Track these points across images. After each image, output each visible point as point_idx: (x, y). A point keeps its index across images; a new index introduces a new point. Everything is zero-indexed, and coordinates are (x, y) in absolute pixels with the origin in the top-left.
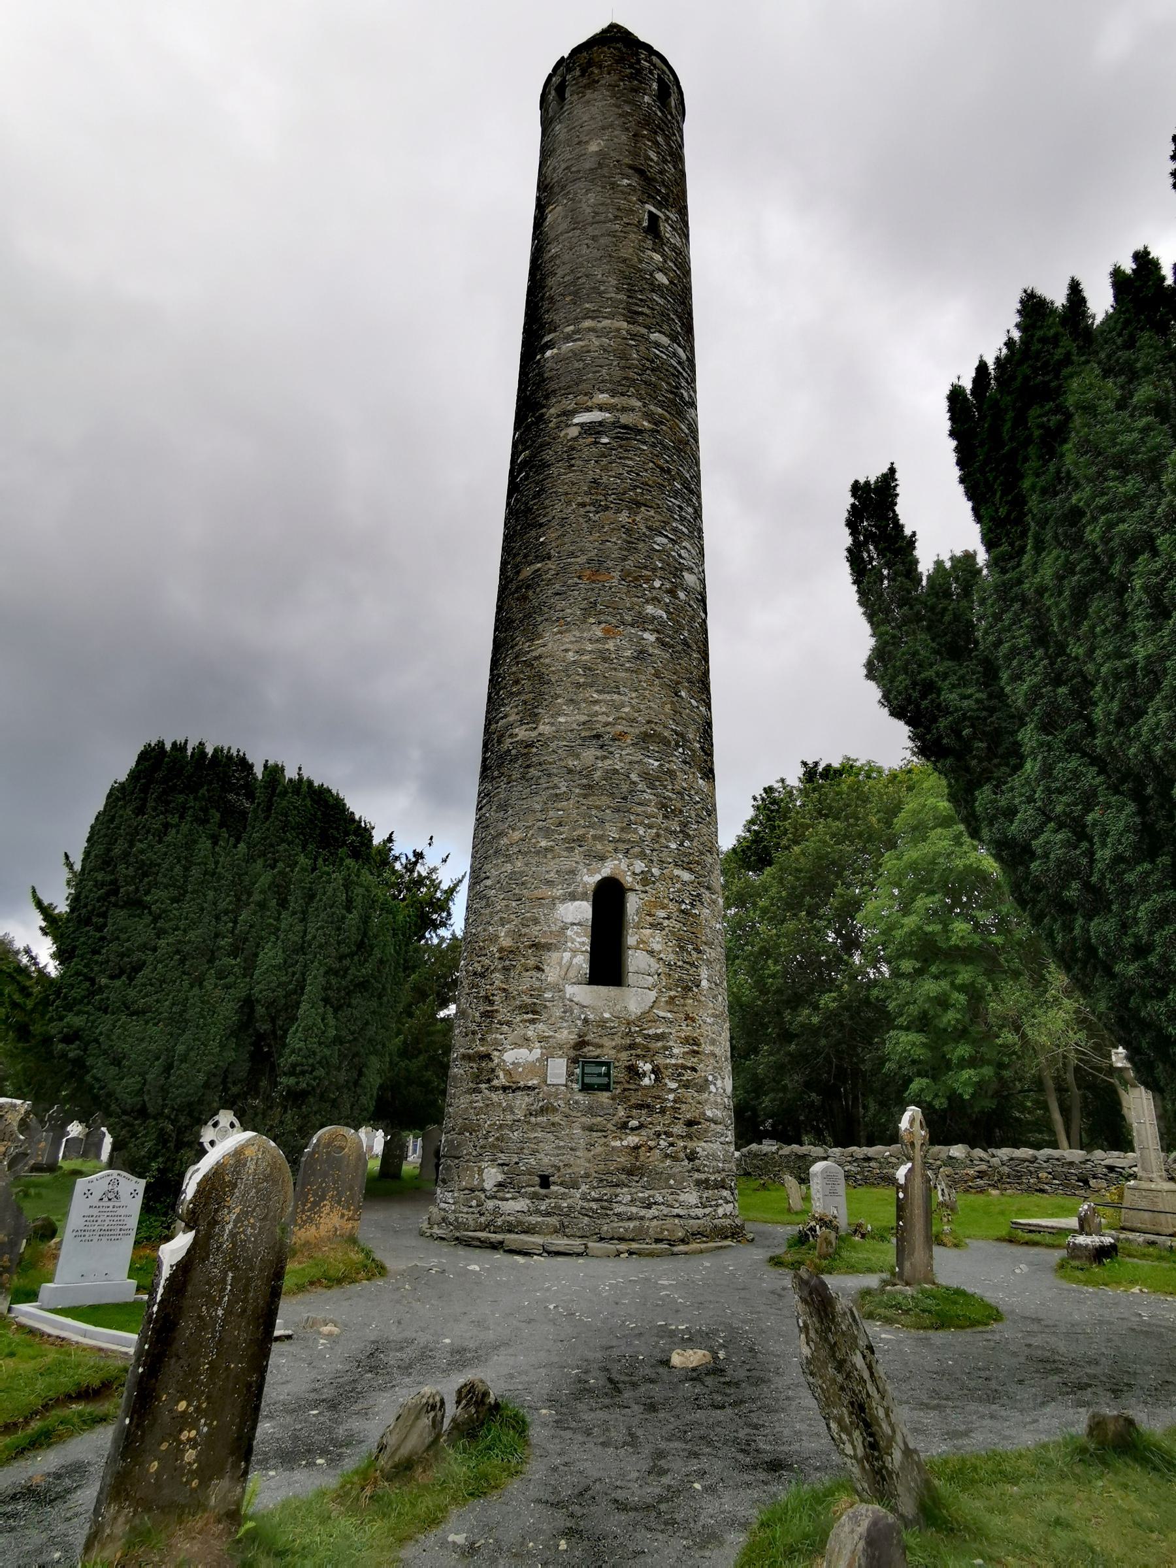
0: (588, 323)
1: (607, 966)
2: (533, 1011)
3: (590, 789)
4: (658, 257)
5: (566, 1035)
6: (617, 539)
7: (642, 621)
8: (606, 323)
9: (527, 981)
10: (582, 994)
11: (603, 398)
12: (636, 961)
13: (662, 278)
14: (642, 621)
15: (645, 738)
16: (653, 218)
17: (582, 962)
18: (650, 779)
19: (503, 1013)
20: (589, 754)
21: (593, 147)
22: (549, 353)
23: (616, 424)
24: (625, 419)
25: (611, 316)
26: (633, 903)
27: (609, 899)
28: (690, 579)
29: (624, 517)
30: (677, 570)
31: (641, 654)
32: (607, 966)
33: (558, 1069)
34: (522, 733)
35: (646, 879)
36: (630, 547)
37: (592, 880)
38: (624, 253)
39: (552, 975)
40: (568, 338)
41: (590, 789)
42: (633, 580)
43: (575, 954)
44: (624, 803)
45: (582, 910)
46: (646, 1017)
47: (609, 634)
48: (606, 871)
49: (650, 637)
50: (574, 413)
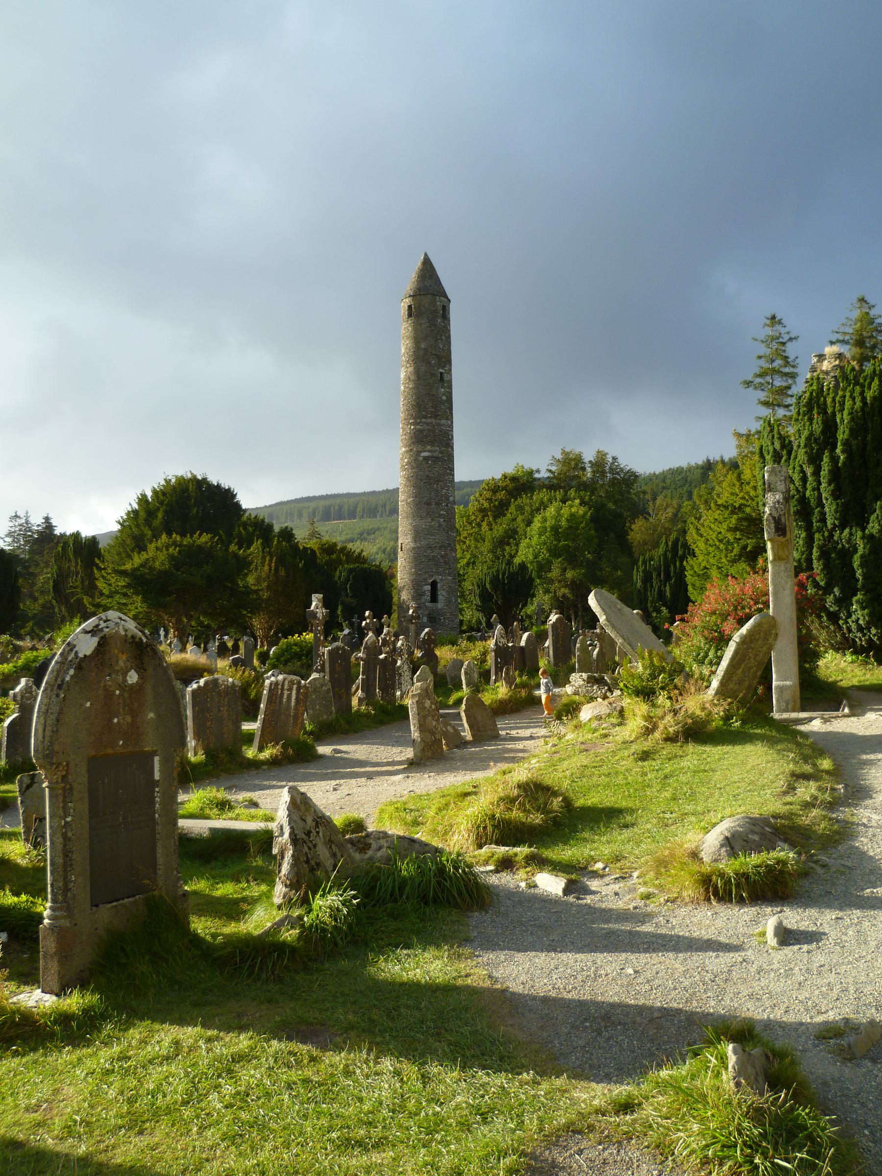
0: (423, 420)
3: (429, 560)
7: (440, 516)
8: (429, 420)
12: (440, 597)
14: (440, 516)
15: (441, 547)
16: (441, 373)
18: (442, 557)
20: (429, 551)
23: (433, 457)
25: (430, 417)
26: (439, 586)
27: (434, 585)
28: (451, 499)
30: (447, 499)
31: (440, 526)
32: (434, 599)
35: (442, 580)
39: (423, 601)
41: (429, 560)
42: (437, 504)
50: (421, 452)
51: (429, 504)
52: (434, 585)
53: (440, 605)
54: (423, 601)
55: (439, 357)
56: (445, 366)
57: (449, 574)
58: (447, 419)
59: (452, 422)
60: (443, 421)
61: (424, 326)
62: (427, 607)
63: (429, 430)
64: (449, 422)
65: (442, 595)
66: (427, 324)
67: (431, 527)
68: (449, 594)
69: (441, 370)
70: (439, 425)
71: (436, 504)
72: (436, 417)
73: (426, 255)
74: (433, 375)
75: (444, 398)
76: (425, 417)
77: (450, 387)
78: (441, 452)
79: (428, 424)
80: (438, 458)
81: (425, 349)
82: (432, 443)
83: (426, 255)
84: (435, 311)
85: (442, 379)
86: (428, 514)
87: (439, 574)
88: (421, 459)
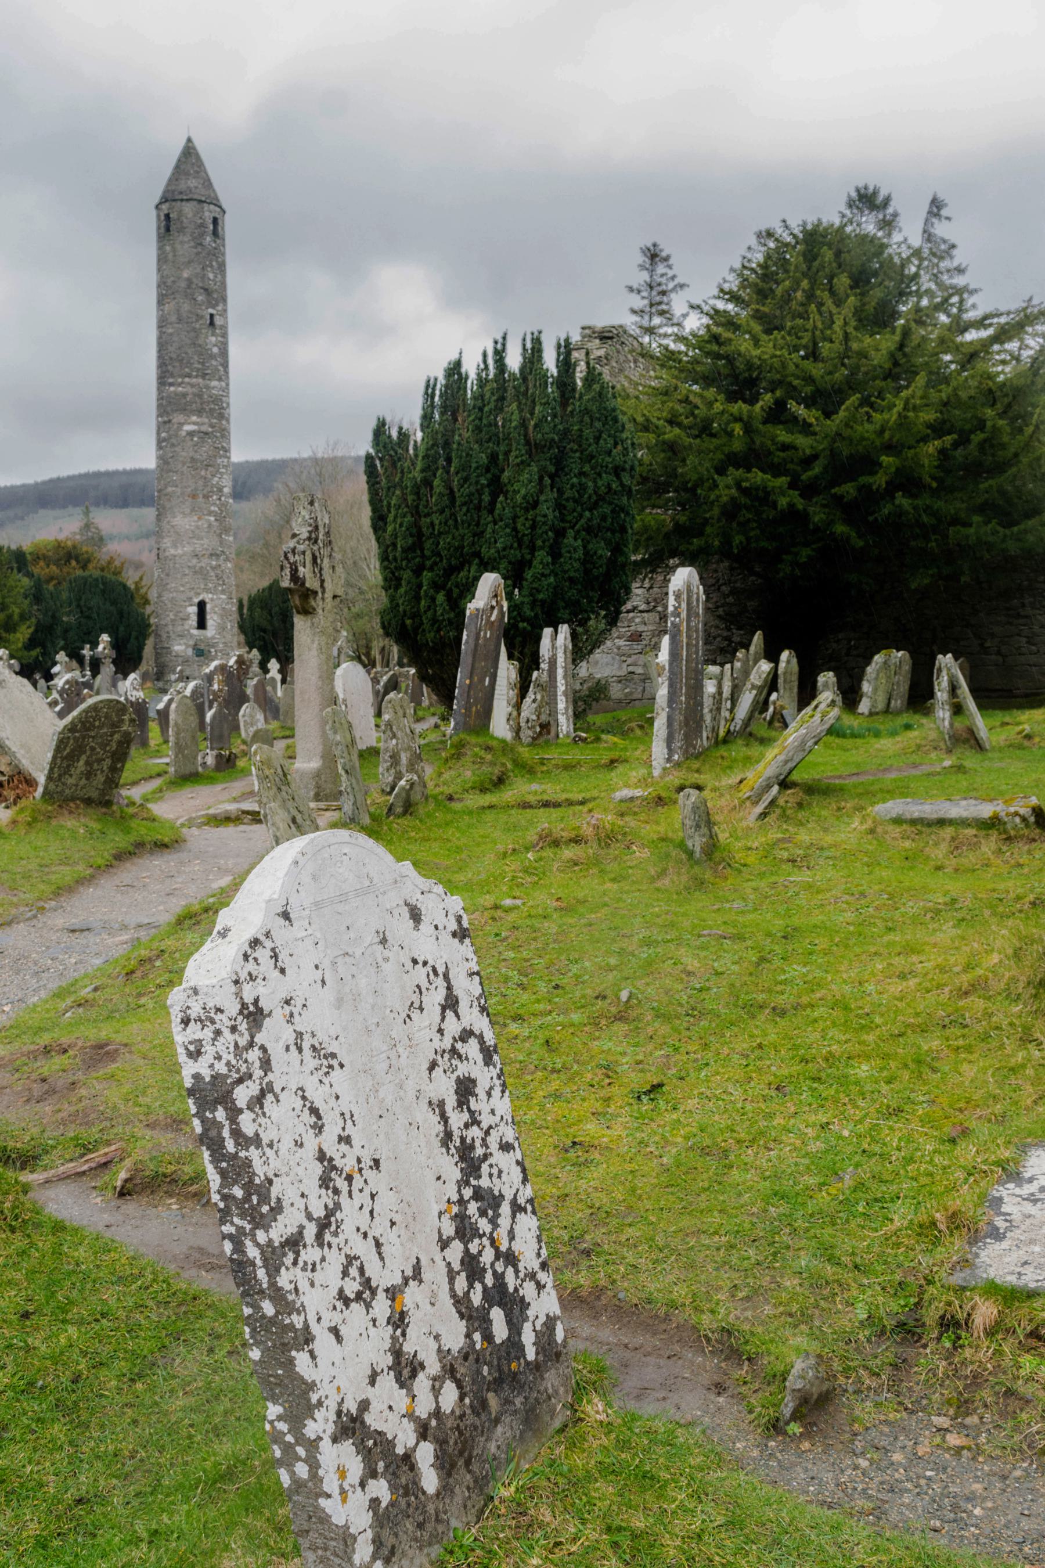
0: (187, 380)
1: (202, 624)
2: (181, 636)
4: (213, 339)
5: (192, 643)
6: (201, 483)
9: (180, 628)
10: (195, 632)
11: (194, 418)
13: (215, 350)
14: (210, 513)
17: (195, 624)
18: (213, 568)
19: (173, 636)
20: (195, 561)
21: (185, 274)
22: (172, 389)
23: (200, 432)
24: (204, 428)
25: (196, 377)
26: (208, 607)
27: (202, 606)
29: (203, 473)
31: (210, 526)
32: (202, 624)
33: (190, 652)
34: (172, 551)
35: (212, 600)
36: (205, 486)
37: (196, 600)
38: (200, 342)
39: (187, 627)
40: (180, 385)
42: (206, 497)
43: (193, 620)
44: (205, 578)
45: (193, 610)
46: (213, 638)
47: (199, 518)
48: (200, 598)
49: (212, 519)
50: (182, 424)
51: (194, 496)
52: (202, 606)
53: (211, 631)
54: (187, 627)
55: (207, 291)
56: (217, 305)
57: (223, 592)
58: (220, 379)
59: (228, 385)
60: (214, 383)
61: (186, 246)
62: (192, 636)
63: (195, 395)
64: (223, 384)
65: (211, 621)
66: (192, 244)
67: (198, 527)
68: (222, 616)
69: (211, 311)
70: (207, 387)
71: (204, 497)
72: (204, 376)
73: (189, 140)
74: (200, 317)
75: (215, 350)
76: (189, 376)
77: (225, 335)
78: (212, 426)
79: (192, 386)
80: (206, 433)
81: (189, 281)
82: (199, 412)
83: (189, 140)
84: (202, 225)
85: (212, 323)
86: (193, 510)
87: (208, 590)
88: (184, 434)
